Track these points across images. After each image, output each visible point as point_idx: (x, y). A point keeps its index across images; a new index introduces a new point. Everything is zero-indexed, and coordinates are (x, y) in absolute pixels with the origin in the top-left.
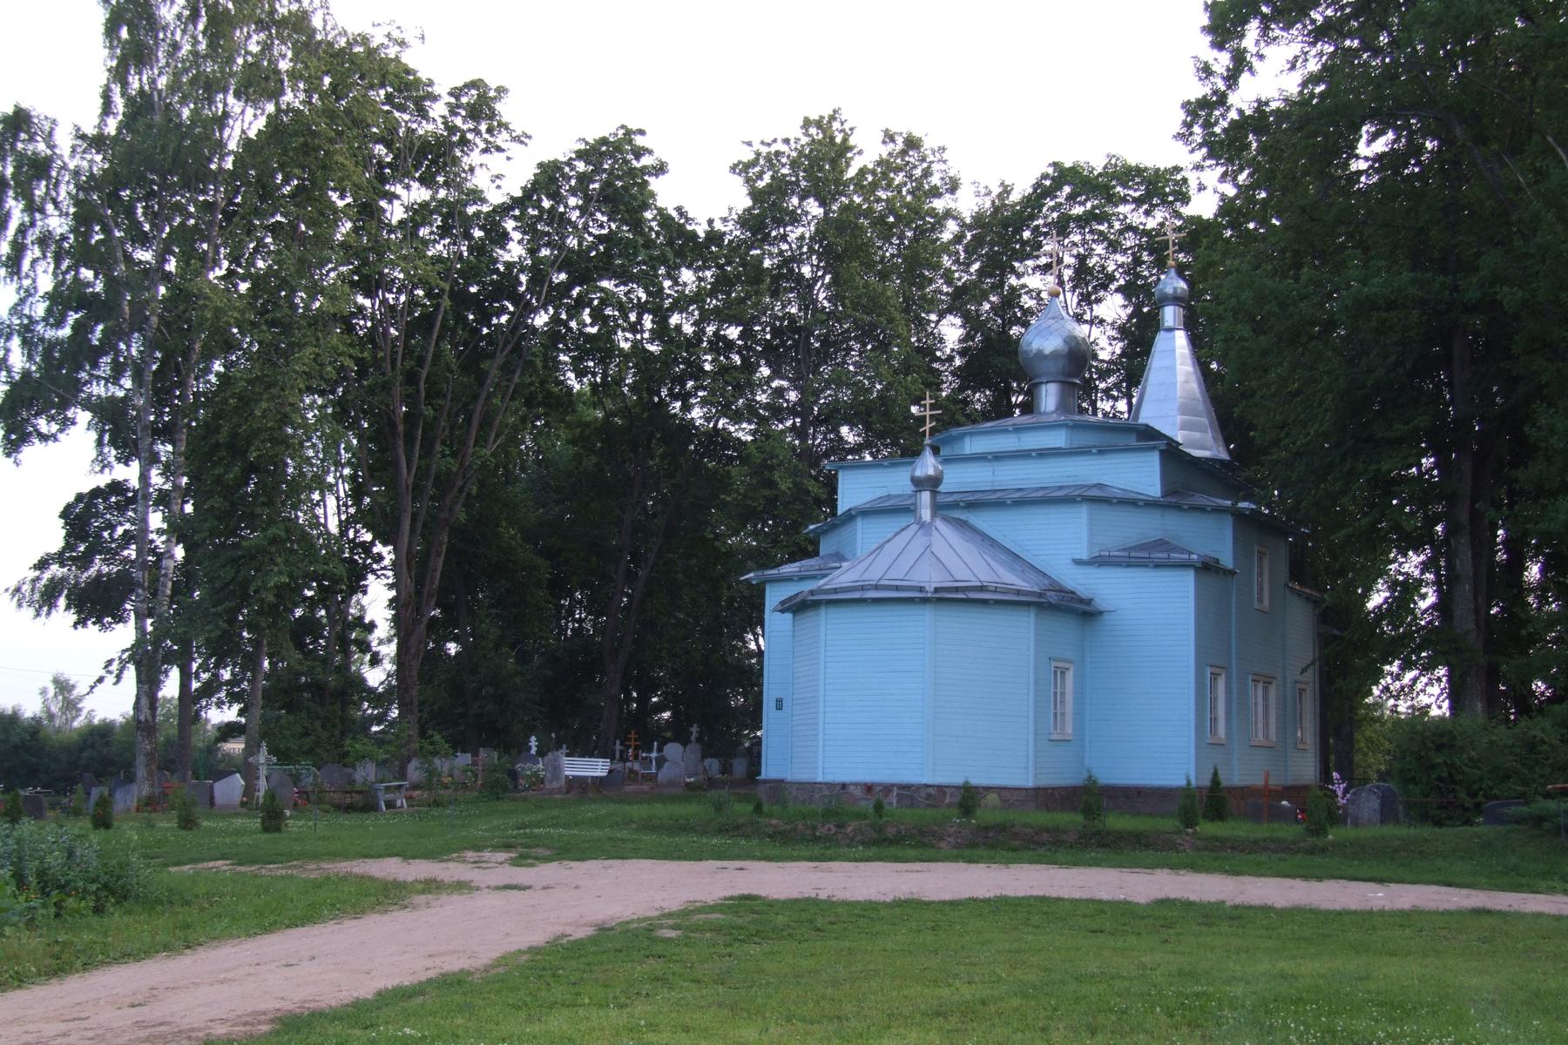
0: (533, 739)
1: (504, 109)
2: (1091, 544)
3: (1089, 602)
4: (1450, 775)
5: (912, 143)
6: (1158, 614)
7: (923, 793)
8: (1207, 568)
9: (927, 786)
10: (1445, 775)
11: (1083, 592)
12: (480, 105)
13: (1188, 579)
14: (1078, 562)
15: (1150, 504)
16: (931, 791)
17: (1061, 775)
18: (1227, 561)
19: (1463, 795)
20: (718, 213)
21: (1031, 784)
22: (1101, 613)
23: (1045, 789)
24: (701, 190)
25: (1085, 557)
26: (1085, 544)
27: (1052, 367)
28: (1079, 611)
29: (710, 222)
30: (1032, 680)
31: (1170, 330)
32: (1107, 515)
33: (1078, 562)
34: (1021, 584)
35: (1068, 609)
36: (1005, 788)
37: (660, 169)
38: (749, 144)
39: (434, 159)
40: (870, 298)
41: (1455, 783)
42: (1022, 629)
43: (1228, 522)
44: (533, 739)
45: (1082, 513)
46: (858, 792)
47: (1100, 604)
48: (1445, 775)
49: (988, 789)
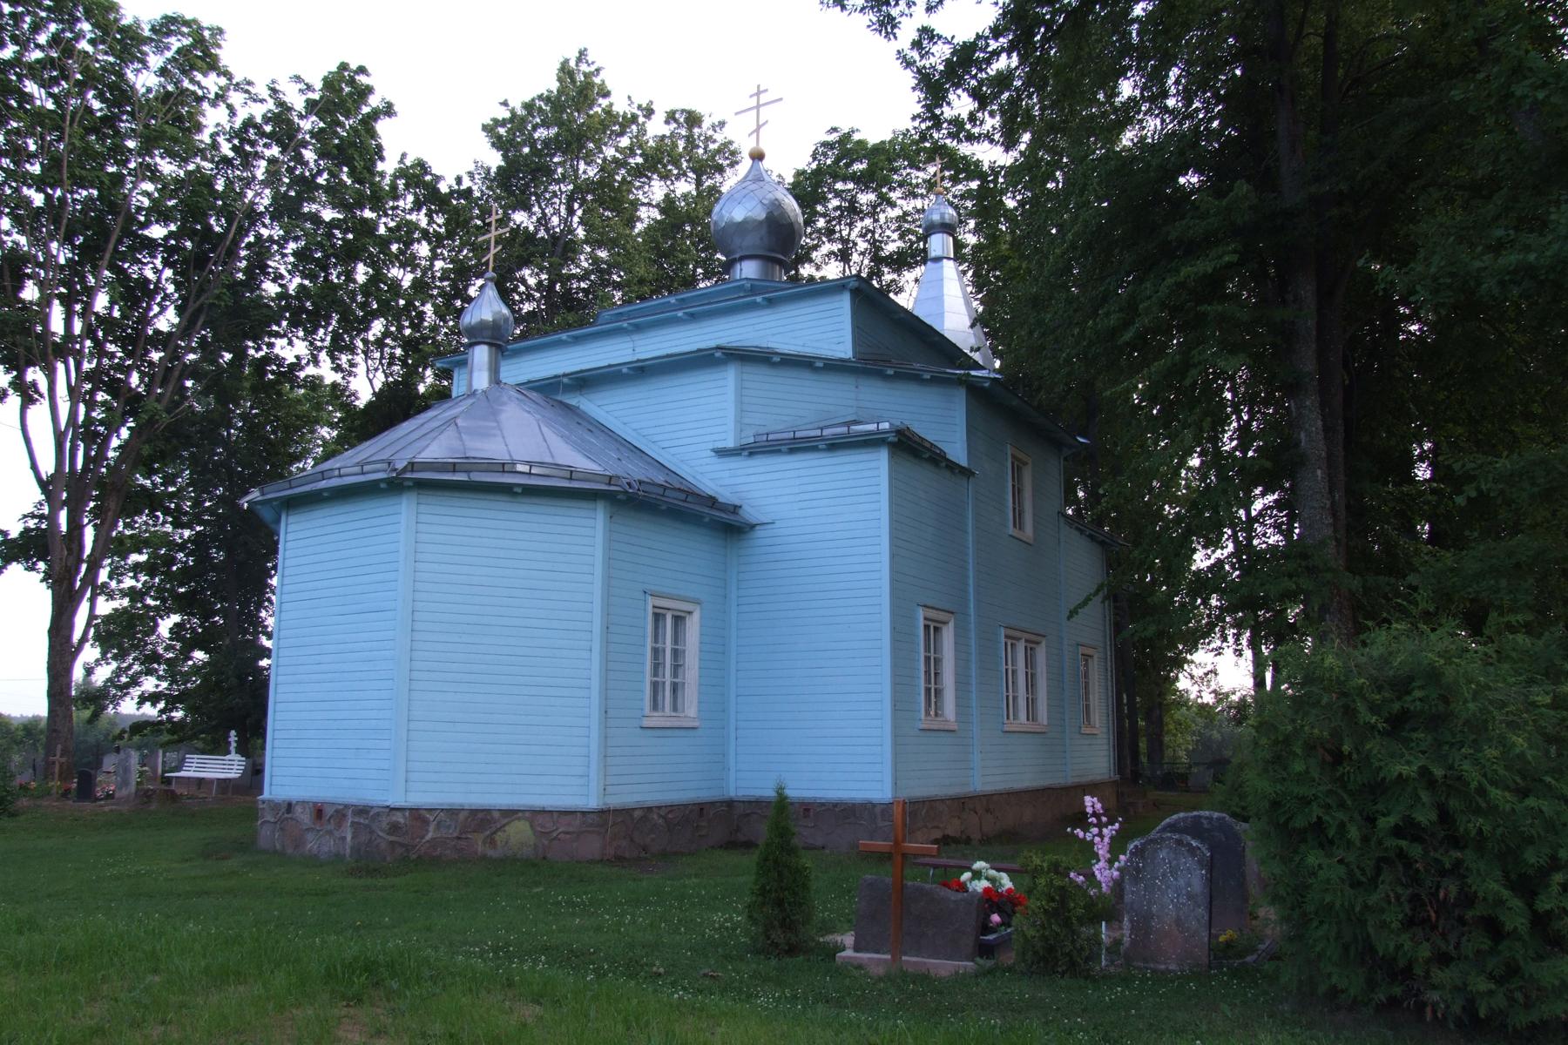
0: (233, 733)
1: (227, 55)
2: (740, 425)
3: (735, 509)
4: (1445, 816)
5: (693, 119)
6: (836, 520)
7: (385, 822)
8: (906, 446)
9: (393, 809)
10: (1425, 816)
11: (725, 496)
12: (201, 52)
13: (878, 464)
14: (722, 453)
15: (833, 367)
16: (399, 818)
17: (660, 779)
18: (957, 452)
19: (1491, 885)
20: (462, 166)
21: (593, 803)
22: (753, 527)
23: (624, 812)
24: (440, 134)
25: (730, 444)
26: (731, 425)
27: (751, 241)
28: (725, 524)
29: (459, 180)
30: (597, 628)
31: (938, 259)
32: (762, 381)
33: (722, 453)
34: (581, 463)
35: (655, 503)
36: (543, 812)
37: (389, 110)
38: (505, 104)
39: (172, 120)
40: (596, 222)
41: (1455, 841)
42: (585, 534)
43: (960, 395)
44: (233, 733)
45: (729, 377)
46: (305, 818)
47: (750, 514)
48: (1425, 816)
49: (510, 814)
